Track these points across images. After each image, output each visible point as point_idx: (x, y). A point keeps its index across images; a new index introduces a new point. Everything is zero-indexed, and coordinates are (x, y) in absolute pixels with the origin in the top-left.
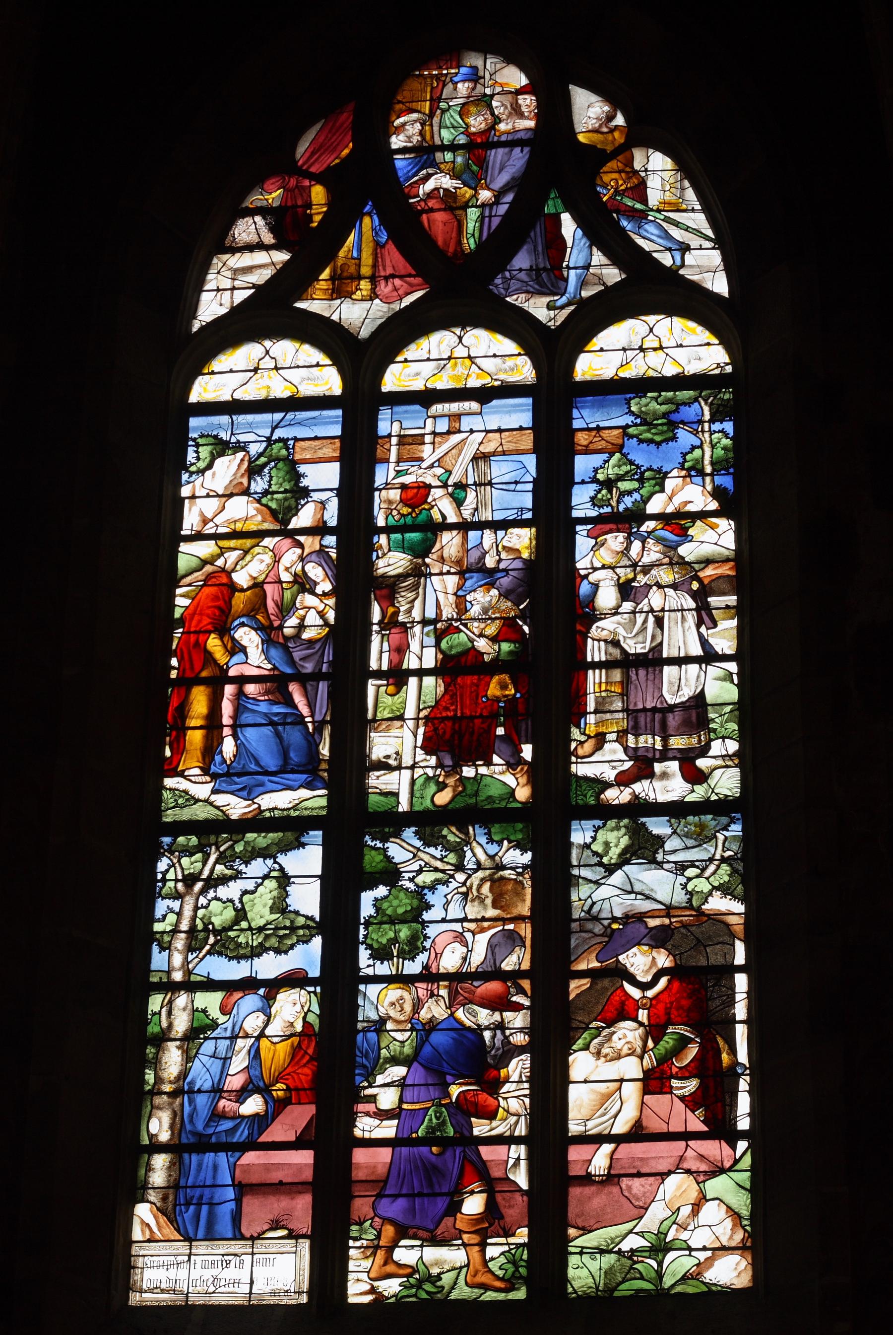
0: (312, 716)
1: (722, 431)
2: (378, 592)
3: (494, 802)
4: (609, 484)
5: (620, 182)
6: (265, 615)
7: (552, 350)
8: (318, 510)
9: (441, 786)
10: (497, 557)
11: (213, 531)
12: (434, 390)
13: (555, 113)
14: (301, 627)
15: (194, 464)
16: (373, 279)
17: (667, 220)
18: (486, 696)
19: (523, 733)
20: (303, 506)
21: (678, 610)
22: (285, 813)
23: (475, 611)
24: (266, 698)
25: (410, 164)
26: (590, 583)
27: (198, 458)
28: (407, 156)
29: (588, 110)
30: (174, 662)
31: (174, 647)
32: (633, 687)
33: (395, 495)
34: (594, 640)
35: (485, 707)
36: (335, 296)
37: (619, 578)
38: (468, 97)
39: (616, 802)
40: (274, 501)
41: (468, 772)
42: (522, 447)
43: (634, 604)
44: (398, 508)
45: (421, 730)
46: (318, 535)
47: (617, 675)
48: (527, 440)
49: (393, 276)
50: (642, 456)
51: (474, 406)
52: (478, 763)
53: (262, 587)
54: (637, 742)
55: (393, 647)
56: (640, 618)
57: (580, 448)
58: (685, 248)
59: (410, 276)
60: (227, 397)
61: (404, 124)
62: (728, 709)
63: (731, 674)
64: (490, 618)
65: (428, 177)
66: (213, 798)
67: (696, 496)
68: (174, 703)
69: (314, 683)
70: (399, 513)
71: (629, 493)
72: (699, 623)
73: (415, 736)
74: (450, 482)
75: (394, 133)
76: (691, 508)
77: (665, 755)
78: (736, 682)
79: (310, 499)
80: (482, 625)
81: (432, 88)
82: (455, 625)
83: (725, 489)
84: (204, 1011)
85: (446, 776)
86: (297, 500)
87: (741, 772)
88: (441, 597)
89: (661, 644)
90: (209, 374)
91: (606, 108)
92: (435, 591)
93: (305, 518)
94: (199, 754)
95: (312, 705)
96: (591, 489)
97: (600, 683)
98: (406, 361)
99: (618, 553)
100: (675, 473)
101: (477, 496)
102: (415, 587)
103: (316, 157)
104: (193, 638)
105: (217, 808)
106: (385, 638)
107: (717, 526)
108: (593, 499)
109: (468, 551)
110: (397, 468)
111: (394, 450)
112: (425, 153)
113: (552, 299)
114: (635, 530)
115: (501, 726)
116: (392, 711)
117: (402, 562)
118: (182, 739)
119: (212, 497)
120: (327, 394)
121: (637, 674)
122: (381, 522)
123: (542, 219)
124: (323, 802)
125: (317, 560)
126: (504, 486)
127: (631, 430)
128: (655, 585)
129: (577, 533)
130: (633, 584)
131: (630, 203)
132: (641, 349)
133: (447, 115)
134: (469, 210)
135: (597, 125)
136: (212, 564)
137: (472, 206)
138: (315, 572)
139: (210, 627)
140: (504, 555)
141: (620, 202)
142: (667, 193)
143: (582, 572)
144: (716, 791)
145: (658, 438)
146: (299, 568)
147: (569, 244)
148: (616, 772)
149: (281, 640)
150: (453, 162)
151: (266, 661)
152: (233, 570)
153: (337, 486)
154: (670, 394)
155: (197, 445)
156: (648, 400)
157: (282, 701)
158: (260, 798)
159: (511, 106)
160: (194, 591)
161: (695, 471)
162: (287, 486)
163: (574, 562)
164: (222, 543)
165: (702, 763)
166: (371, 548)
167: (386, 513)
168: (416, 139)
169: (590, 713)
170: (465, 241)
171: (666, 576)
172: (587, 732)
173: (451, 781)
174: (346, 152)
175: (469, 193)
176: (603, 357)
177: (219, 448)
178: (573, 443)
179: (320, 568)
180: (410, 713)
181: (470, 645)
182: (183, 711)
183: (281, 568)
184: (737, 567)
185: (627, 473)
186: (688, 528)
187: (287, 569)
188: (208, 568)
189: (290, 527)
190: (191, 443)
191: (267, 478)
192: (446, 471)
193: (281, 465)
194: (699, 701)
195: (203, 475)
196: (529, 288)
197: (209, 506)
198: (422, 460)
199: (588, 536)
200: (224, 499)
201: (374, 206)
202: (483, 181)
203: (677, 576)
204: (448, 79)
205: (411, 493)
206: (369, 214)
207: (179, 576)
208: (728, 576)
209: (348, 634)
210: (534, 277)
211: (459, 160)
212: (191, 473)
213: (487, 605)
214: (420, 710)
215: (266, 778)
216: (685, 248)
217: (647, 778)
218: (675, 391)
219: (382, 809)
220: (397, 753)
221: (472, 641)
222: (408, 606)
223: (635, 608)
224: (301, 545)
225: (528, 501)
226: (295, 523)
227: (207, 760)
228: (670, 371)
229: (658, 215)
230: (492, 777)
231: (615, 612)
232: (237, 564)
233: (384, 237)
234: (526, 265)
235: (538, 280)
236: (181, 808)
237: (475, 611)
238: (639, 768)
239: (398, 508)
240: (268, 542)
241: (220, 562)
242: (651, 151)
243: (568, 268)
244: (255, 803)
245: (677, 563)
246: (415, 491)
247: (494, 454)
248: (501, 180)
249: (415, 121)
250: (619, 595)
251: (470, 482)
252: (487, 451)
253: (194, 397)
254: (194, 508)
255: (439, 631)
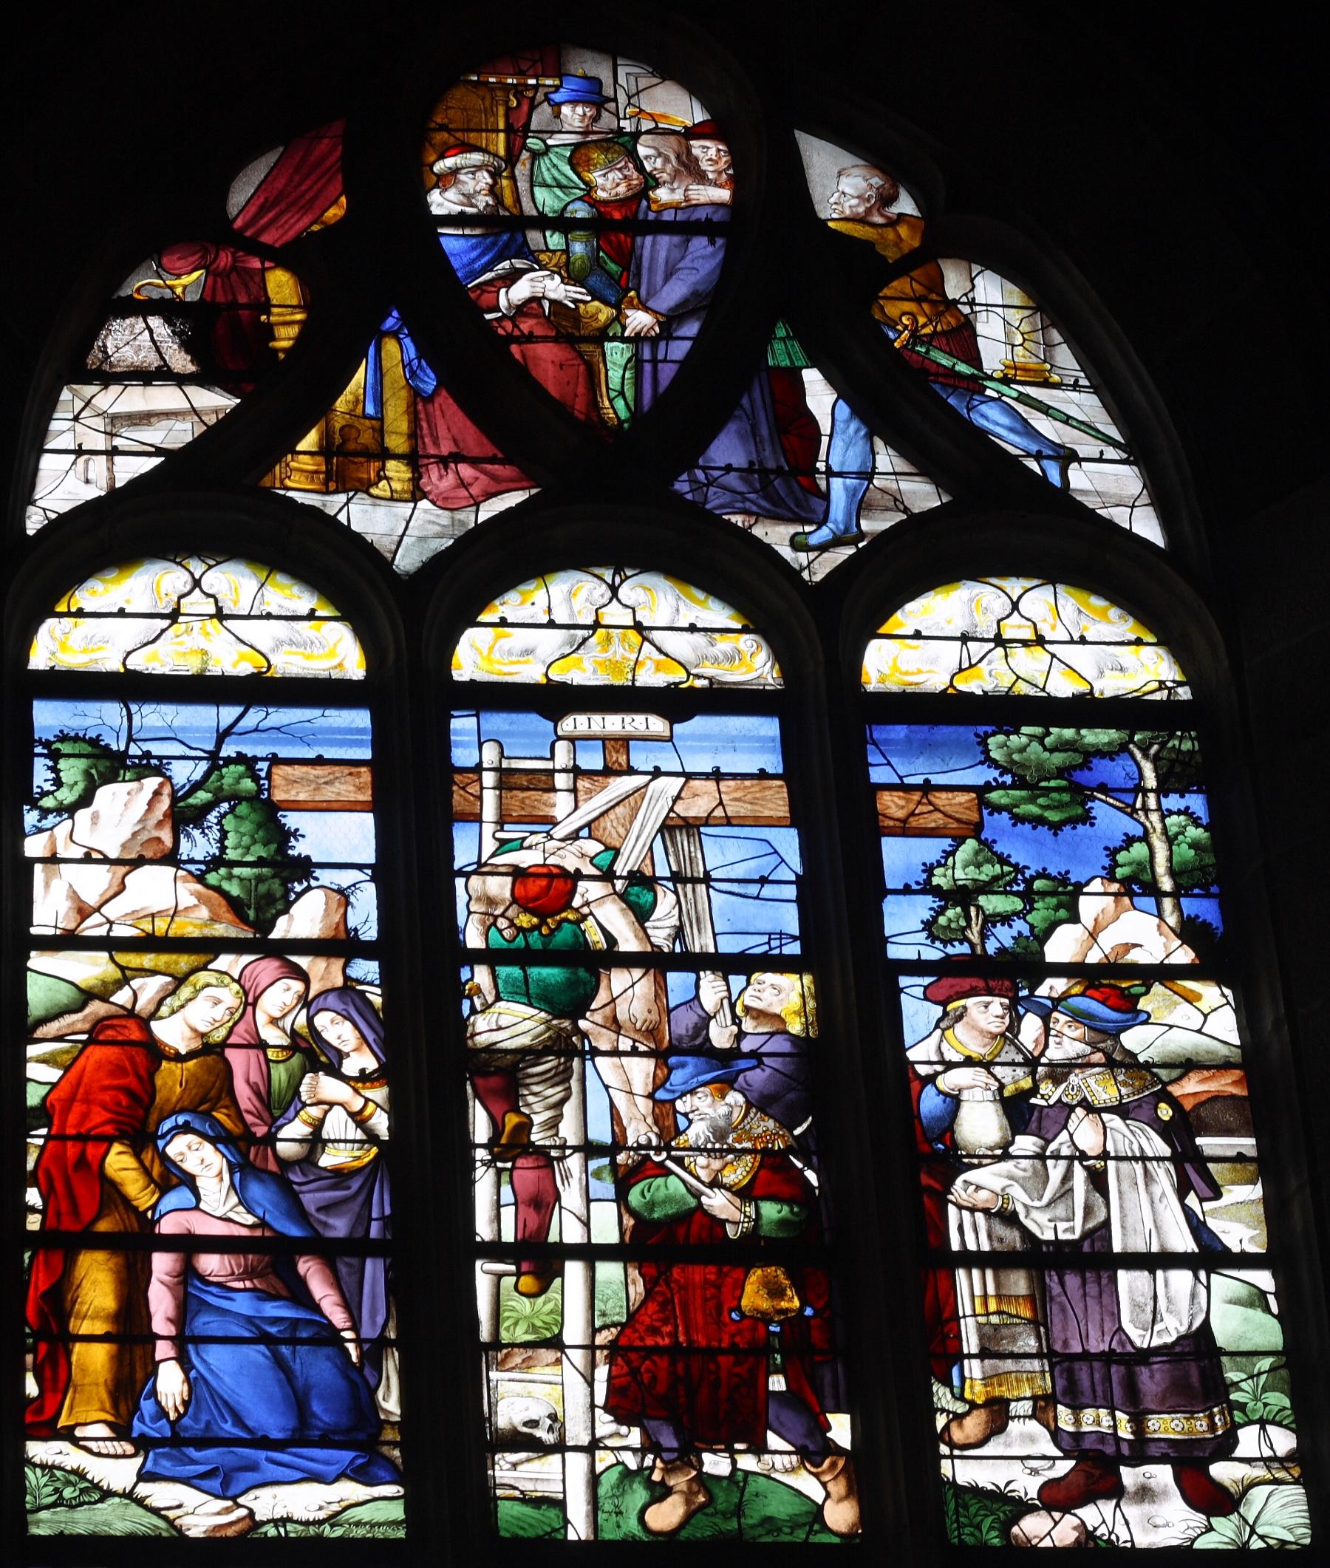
0: (355, 1327)
1: (1185, 812)
2: (479, 1081)
3: (779, 1530)
4: (963, 896)
5: (922, 320)
6: (232, 1113)
7: (818, 628)
8: (334, 905)
9: (659, 1491)
10: (735, 1029)
11: (102, 931)
12: (564, 686)
13: (771, 187)
14: (316, 1141)
15: (48, 793)
16: (413, 460)
17: (1022, 398)
18: (738, 1308)
19: (828, 1391)
20: (299, 895)
21: (1135, 1158)
22: (312, 1530)
23: (697, 1132)
24: (248, 1284)
25: (474, 248)
26: (940, 1092)
27: (58, 783)
28: (467, 232)
29: (840, 186)
30: (33, 1196)
31: (30, 1165)
32: (1055, 1308)
33: (500, 887)
34: (960, 1207)
35: (739, 1332)
36: (332, 486)
37: (1002, 1087)
38: (585, 133)
39: (1047, 1543)
40: (235, 881)
41: (716, 1464)
42: (767, 813)
43: (1041, 1142)
44: (510, 913)
45: (602, 1373)
46: (338, 956)
47: (1019, 1283)
48: (776, 801)
49: (457, 458)
50: (1024, 850)
51: (657, 725)
52: (738, 1446)
53: (222, 1054)
54: (1077, 1422)
55: (523, 1195)
56: (1056, 1171)
57: (891, 823)
58: (1067, 457)
59: (492, 460)
60: (114, 665)
61: (455, 171)
62: (1265, 1363)
63: (1263, 1294)
64: (731, 1150)
65: (512, 278)
66: (143, 1490)
67: (1146, 936)
68: (40, 1282)
69: (354, 1261)
70: (512, 924)
71: (1006, 919)
72: (1183, 1189)
73: (590, 1383)
74: (621, 868)
75: (436, 186)
76: (1136, 957)
77: (1141, 1452)
78: (1275, 1309)
79: (313, 883)
80: (716, 1164)
81: (508, 110)
82: (657, 1159)
83: (1206, 925)
85: (667, 1471)
86: (286, 882)
87: (1308, 1494)
88: (621, 1101)
89: (1107, 1223)
90: (69, 614)
91: (876, 181)
92: (607, 1087)
93: (305, 917)
94: (105, 1396)
95: (354, 1306)
96: (923, 907)
97: (985, 1297)
98: (503, 623)
99: (994, 1037)
100: (1096, 885)
101: (679, 902)
102: (562, 1076)
103: (271, 215)
104: (71, 1150)
105: (156, 1511)
106: (505, 1177)
107: (1199, 997)
108: (928, 926)
109: (669, 1011)
110: (499, 835)
111: (490, 798)
112: (506, 230)
113: (800, 529)
114: (1025, 993)
115: (777, 1372)
116: (534, 1328)
117: (528, 1025)
118: (62, 1362)
119: (96, 862)
120: (336, 675)
121: (1062, 1283)
122: (474, 939)
123: (764, 375)
124: (396, 1511)
125: (340, 1007)
126: (735, 887)
127: (994, 796)
128: (1079, 1104)
129: (901, 990)
130: (1033, 1101)
131: (945, 361)
132: (999, 641)
133: (544, 163)
134: (608, 345)
135: (861, 209)
136: (105, 999)
137: (614, 339)
138: (337, 1030)
139: (108, 1129)
140: (748, 1025)
141: (925, 358)
142: (1019, 350)
143: (923, 1070)
144: (1260, 1530)
145: (1053, 816)
146: (302, 1019)
147: (825, 427)
148: (1038, 1481)
149: (272, 1166)
150: (566, 251)
151: (241, 1209)
152: (154, 1015)
153: (372, 860)
154: (1069, 733)
155: (55, 756)
156: (1024, 740)
157: (284, 1293)
158: (251, 1495)
159: (678, 157)
160: (67, 1052)
161: (1138, 886)
162: (259, 851)
163: (901, 1048)
164: (123, 958)
165: (1222, 1471)
166: (458, 991)
167: (483, 922)
168: (483, 201)
169: (970, 1356)
170: (607, 403)
171: (1103, 1090)
172: (968, 1395)
173: (679, 1481)
174: (334, 213)
175: (605, 313)
176: (921, 646)
177: (103, 764)
178: (874, 813)
179: (348, 1024)
180: (574, 1332)
181: (692, 1202)
182: (60, 1301)
183: (261, 1019)
184: (1248, 1080)
185: (995, 879)
186: (1138, 997)
187: (274, 1021)
188: (96, 1008)
189: (276, 934)
190: (38, 750)
191: (215, 834)
192: (607, 848)
193: (243, 809)
194: (1200, 1343)
195: (71, 817)
196: (748, 505)
197: (93, 882)
198: (554, 823)
199: (926, 998)
200: (123, 869)
201: (404, 320)
202: (632, 293)
203: (1124, 1091)
204: (540, 96)
205: (535, 887)
206: (394, 334)
207: (30, 1020)
208: (1233, 1096)
209: (422, 1164)
210: (758, 485)
211: (578, 248)
212: (45, 812)
213: (722, 1123)
214: (595, 1331)
215: (261, 1455)
216: (1067, 457)
217: (1107, 1496)
218: (1078, 727)
219: (531, 1533)
220: (553, 1417)
221: (697, 1195)
222: (549, 1114)
223: (1044, 1149)
224: (303, 976)
225: (789, 919)
226: (282, 929)
227: (123, 1409)
228: (1063, 687)
229: (1004, 389)
230: (768, 1477)
231: (1004, 1153)
232: (160, 1003)
233: (429, 383)
234: (739, 460)
235: (765, 490)
236: (71, 1507)
237: (697, 1132)
238: (1089, 1476)
239: (510, 913)
240: (225, 962)
241: (122, 997)
242: (976, 268)
243: (830, 473)
244: (239, 1506)
245: (1121, 1065)
246: (543, 882)
247: (707, 821)
248: (672, 294)
249: (479, 168)
250: (1005, 1121)
251: (662, 871)
252: (692, 814)
253: (39, 658)
254: (55, 883)
255: (621, 1171)
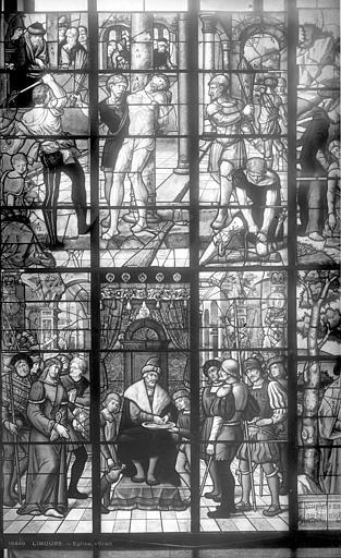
27: (305, 39)
84: (326, 373)
241: (320, 105)
